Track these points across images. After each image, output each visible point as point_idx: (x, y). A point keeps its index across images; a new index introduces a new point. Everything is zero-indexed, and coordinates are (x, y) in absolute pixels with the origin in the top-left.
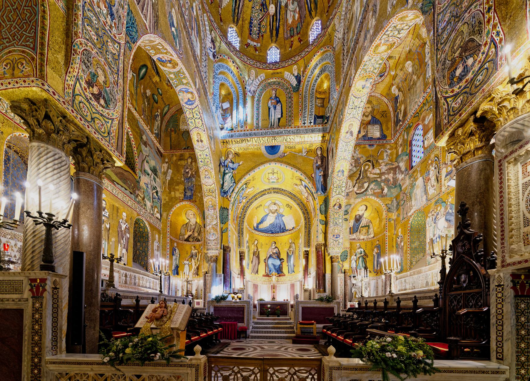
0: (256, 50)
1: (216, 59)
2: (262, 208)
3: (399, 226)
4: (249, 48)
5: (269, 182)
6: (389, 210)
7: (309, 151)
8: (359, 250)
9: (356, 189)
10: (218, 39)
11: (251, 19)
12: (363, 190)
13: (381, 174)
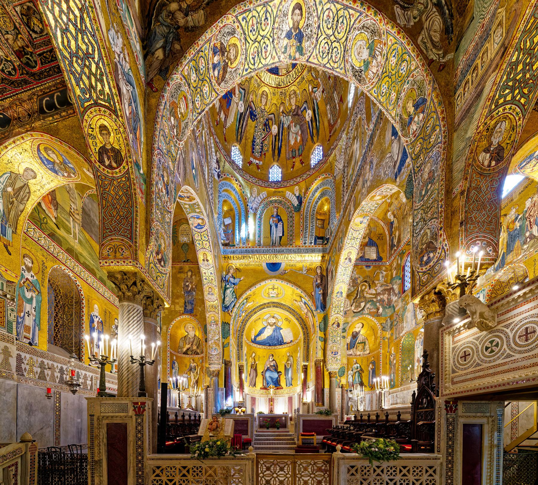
0: (258, 168)
1: (221, 179)
2: (260, 321)
3: (392, 345)
4: (251, 166)
5: (269, 297)
6: (384, 329)
7: (309, 270)
8: (356, 366)
9: (353, 308)
10: (223, 160)
11: (254, 138)
12: (360, 309)
13: (377, 294)
